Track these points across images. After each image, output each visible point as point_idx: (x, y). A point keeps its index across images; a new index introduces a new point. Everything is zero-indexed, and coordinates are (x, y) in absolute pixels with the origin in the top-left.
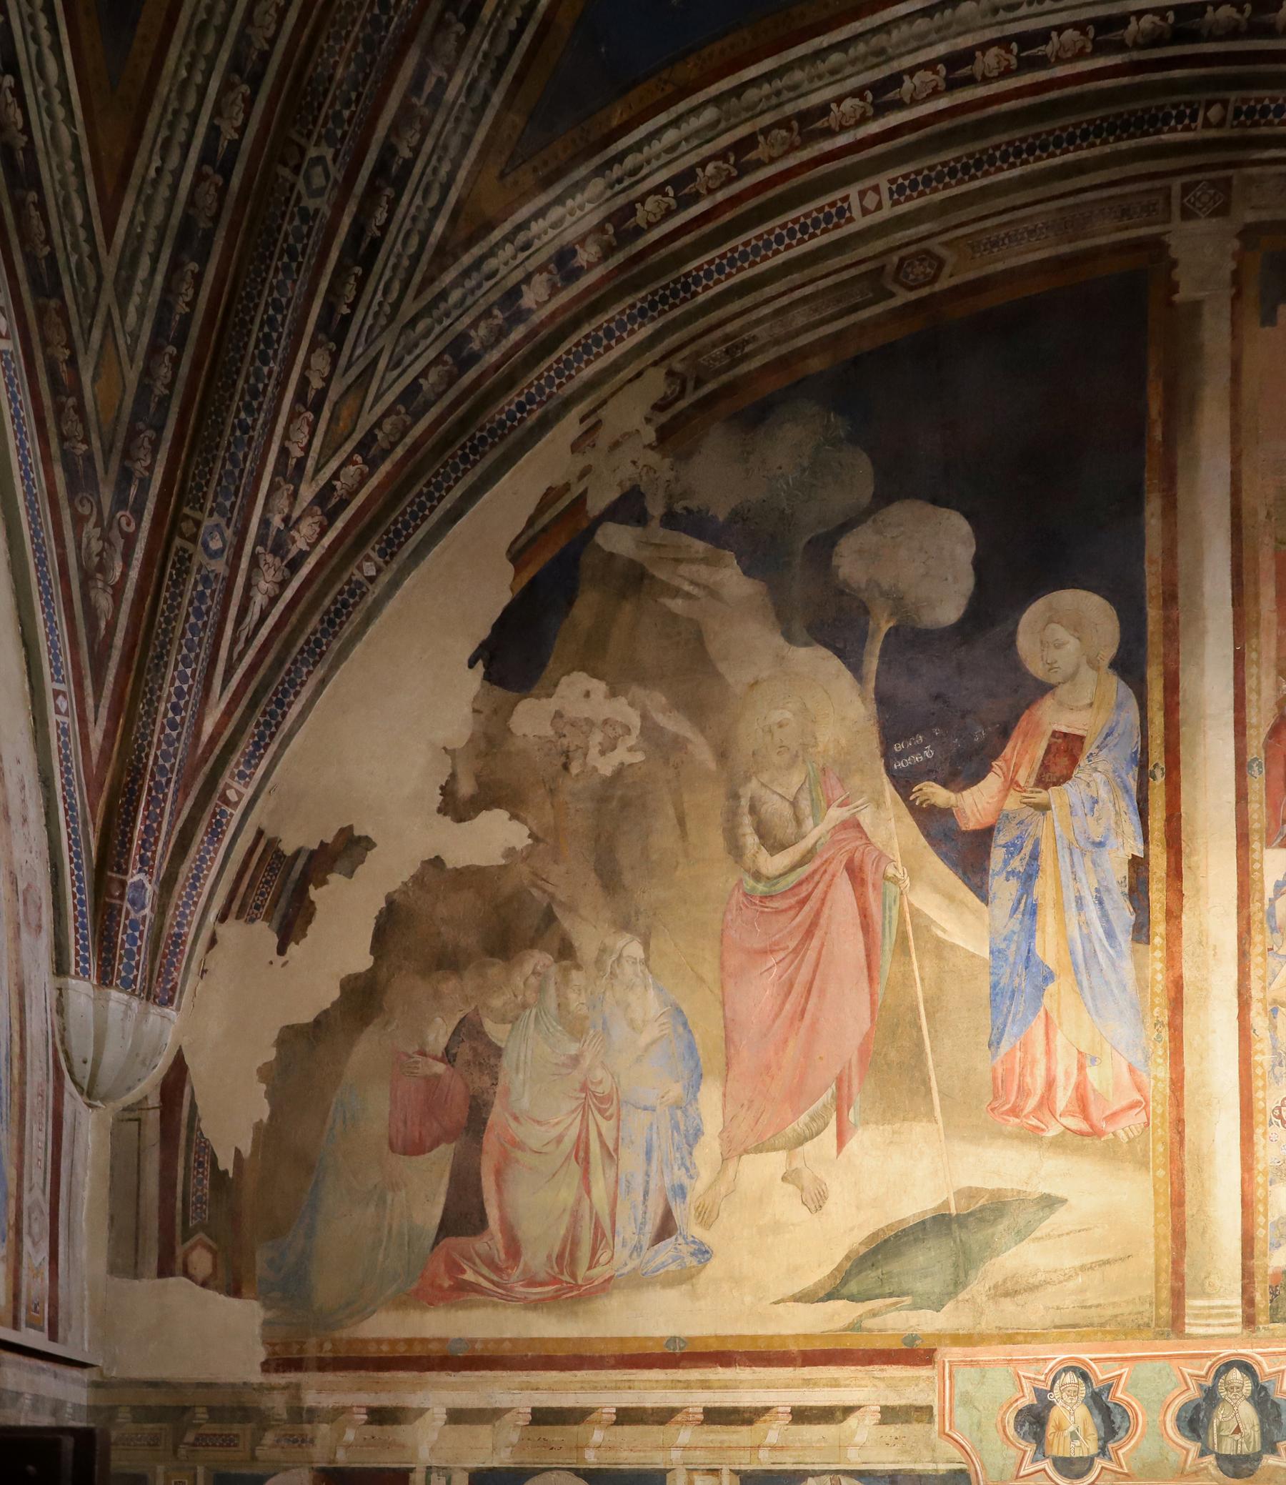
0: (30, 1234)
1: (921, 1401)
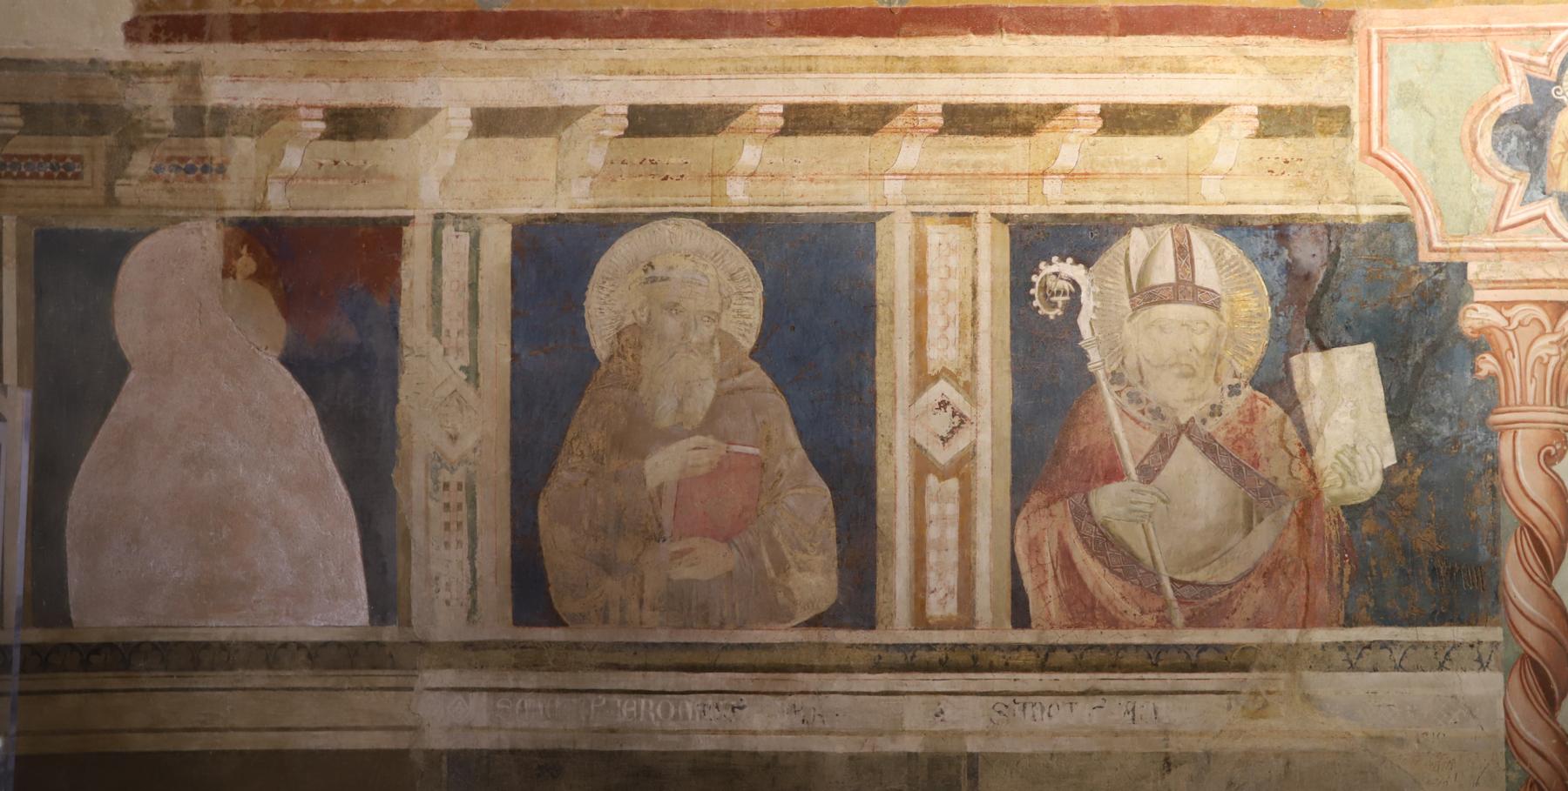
1: (1328, 99)
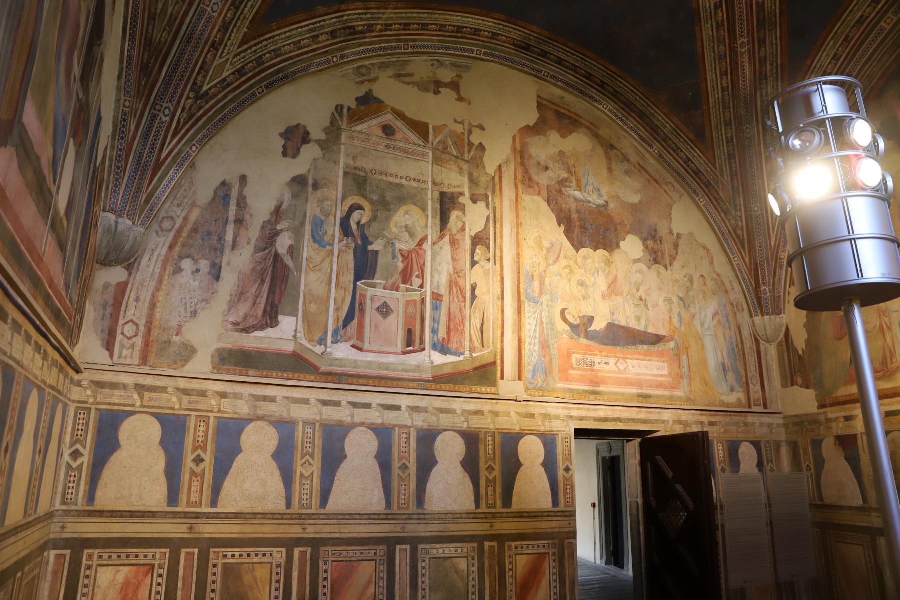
0: (752, 383)
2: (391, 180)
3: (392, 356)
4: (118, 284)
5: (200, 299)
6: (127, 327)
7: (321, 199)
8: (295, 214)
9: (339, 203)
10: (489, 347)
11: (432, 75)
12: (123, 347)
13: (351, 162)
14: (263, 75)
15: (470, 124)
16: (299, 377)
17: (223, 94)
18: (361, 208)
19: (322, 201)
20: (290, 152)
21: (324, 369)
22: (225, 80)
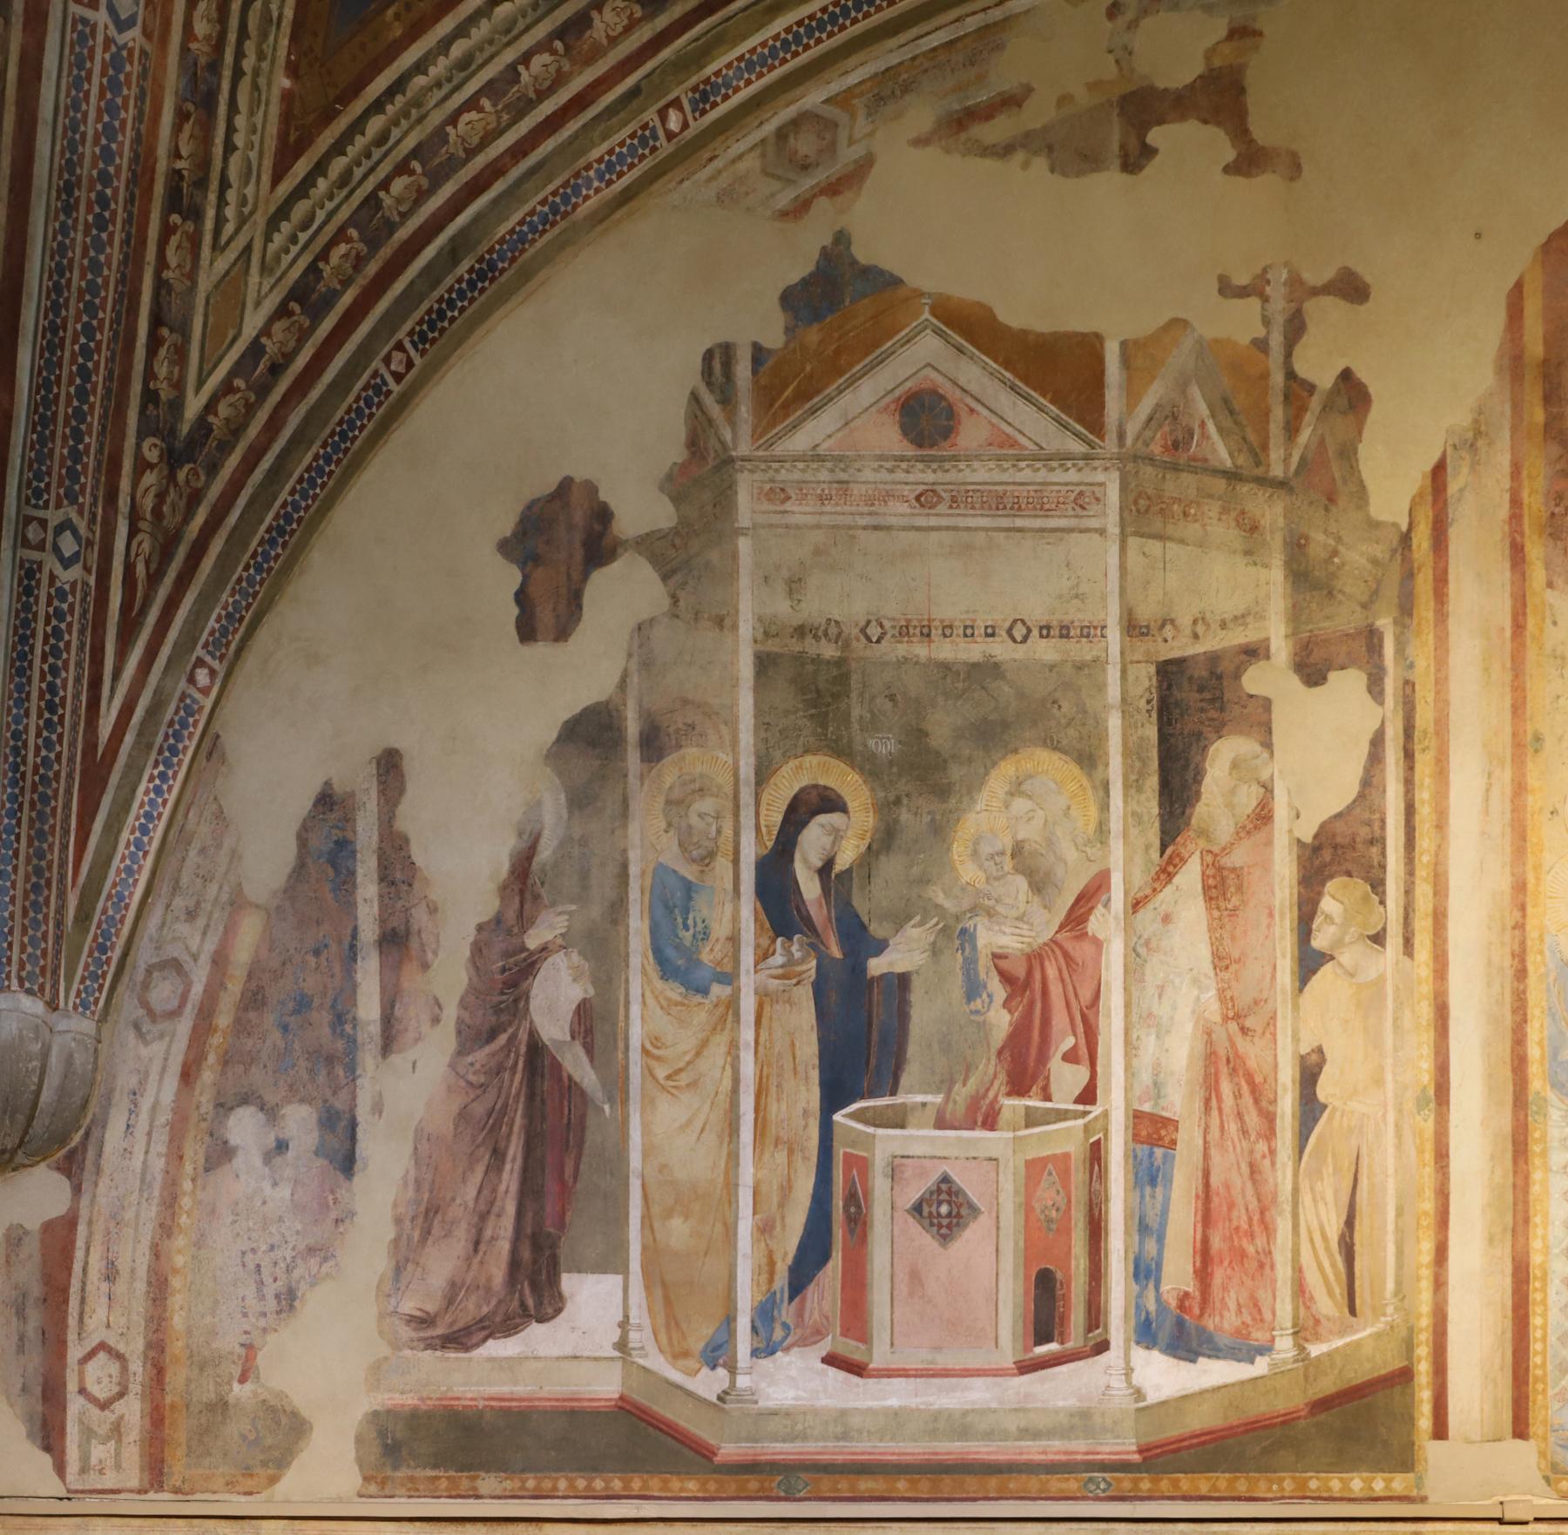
2: (945, 651)
3: (978, 1382)
4: (48, 1227)
5: (302, 1247)
6: (91, 1367)
7: (676, 794)
8: (584, 875)
9: (747, 796)
10: (1378, 1312)
11: (1109, 70)
12: (88, 1433)
13: (781, 607)
14: (399, 286)
15: (1295, 281)
16: (643, 1487)
17: (262, 416)
18: (829, 802)
19: (679, 803)
20: (545, 616)
21: (729, 1450)
22: (256, 349)
